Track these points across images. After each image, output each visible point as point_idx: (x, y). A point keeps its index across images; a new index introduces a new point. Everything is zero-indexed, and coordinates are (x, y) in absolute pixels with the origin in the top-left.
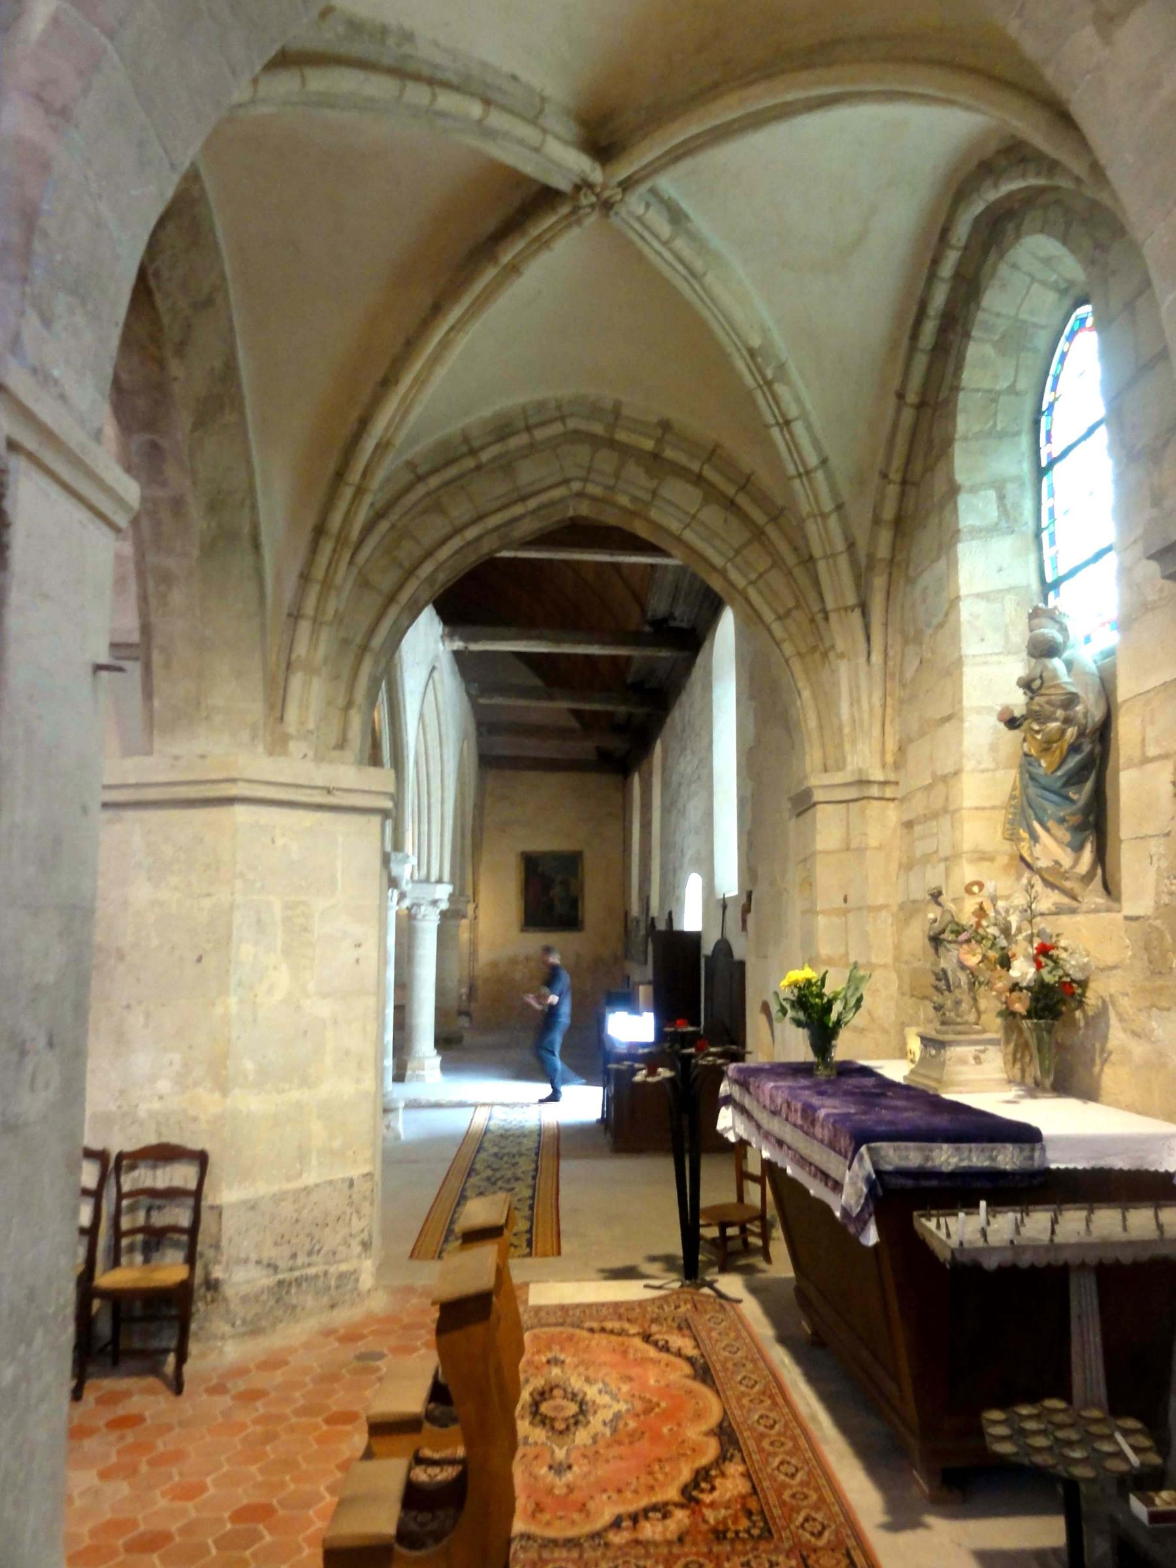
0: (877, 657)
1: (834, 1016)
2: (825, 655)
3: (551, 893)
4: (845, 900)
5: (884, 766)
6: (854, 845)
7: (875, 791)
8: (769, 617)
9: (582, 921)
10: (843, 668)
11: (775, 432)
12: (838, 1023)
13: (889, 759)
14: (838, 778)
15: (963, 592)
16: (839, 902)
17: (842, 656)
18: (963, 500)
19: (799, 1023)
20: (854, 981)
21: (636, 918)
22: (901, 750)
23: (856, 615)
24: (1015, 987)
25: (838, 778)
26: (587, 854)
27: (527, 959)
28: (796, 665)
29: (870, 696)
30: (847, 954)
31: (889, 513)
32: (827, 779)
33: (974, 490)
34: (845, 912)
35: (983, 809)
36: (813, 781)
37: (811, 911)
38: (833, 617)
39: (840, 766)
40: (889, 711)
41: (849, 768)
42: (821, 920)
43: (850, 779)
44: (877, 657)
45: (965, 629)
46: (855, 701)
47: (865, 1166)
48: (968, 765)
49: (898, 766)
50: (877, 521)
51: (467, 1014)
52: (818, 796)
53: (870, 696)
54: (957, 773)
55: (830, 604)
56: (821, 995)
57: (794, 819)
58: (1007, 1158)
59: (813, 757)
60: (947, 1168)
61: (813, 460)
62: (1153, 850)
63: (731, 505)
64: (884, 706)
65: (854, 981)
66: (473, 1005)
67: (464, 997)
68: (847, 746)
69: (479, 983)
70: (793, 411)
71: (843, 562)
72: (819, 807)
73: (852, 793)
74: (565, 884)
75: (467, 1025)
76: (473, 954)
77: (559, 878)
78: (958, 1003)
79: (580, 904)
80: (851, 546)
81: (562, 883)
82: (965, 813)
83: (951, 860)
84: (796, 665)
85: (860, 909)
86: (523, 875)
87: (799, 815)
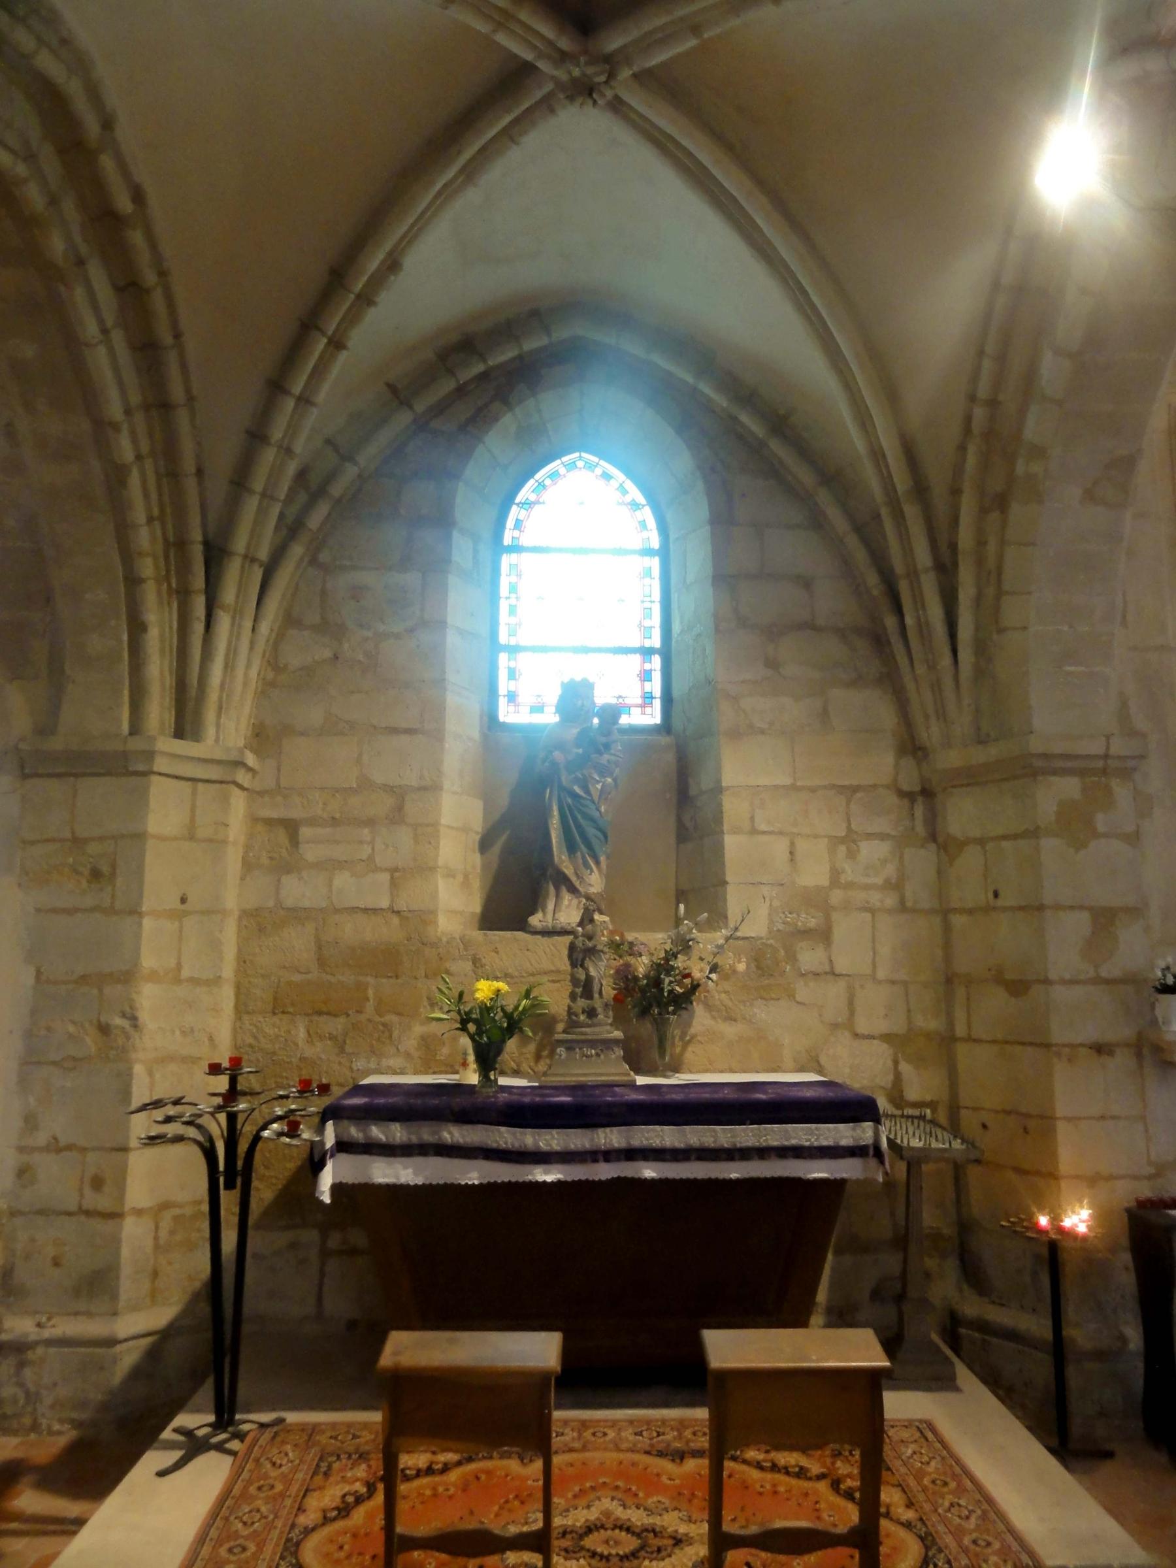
0: (264, 628)
4: (183, 900)
6: (201, 833)
16: (177, 904)
29: (248, 666)
30: (179, 966)
34: (177, 916)
35: (452, 828)
42: (147, 923)
46: (229, 666)
52: (160, 764)
53: (248, 666)
62: (766, 894)
72: (155, 779)
73: (214, 773)
82: (442, 830)
85: (208, 912)
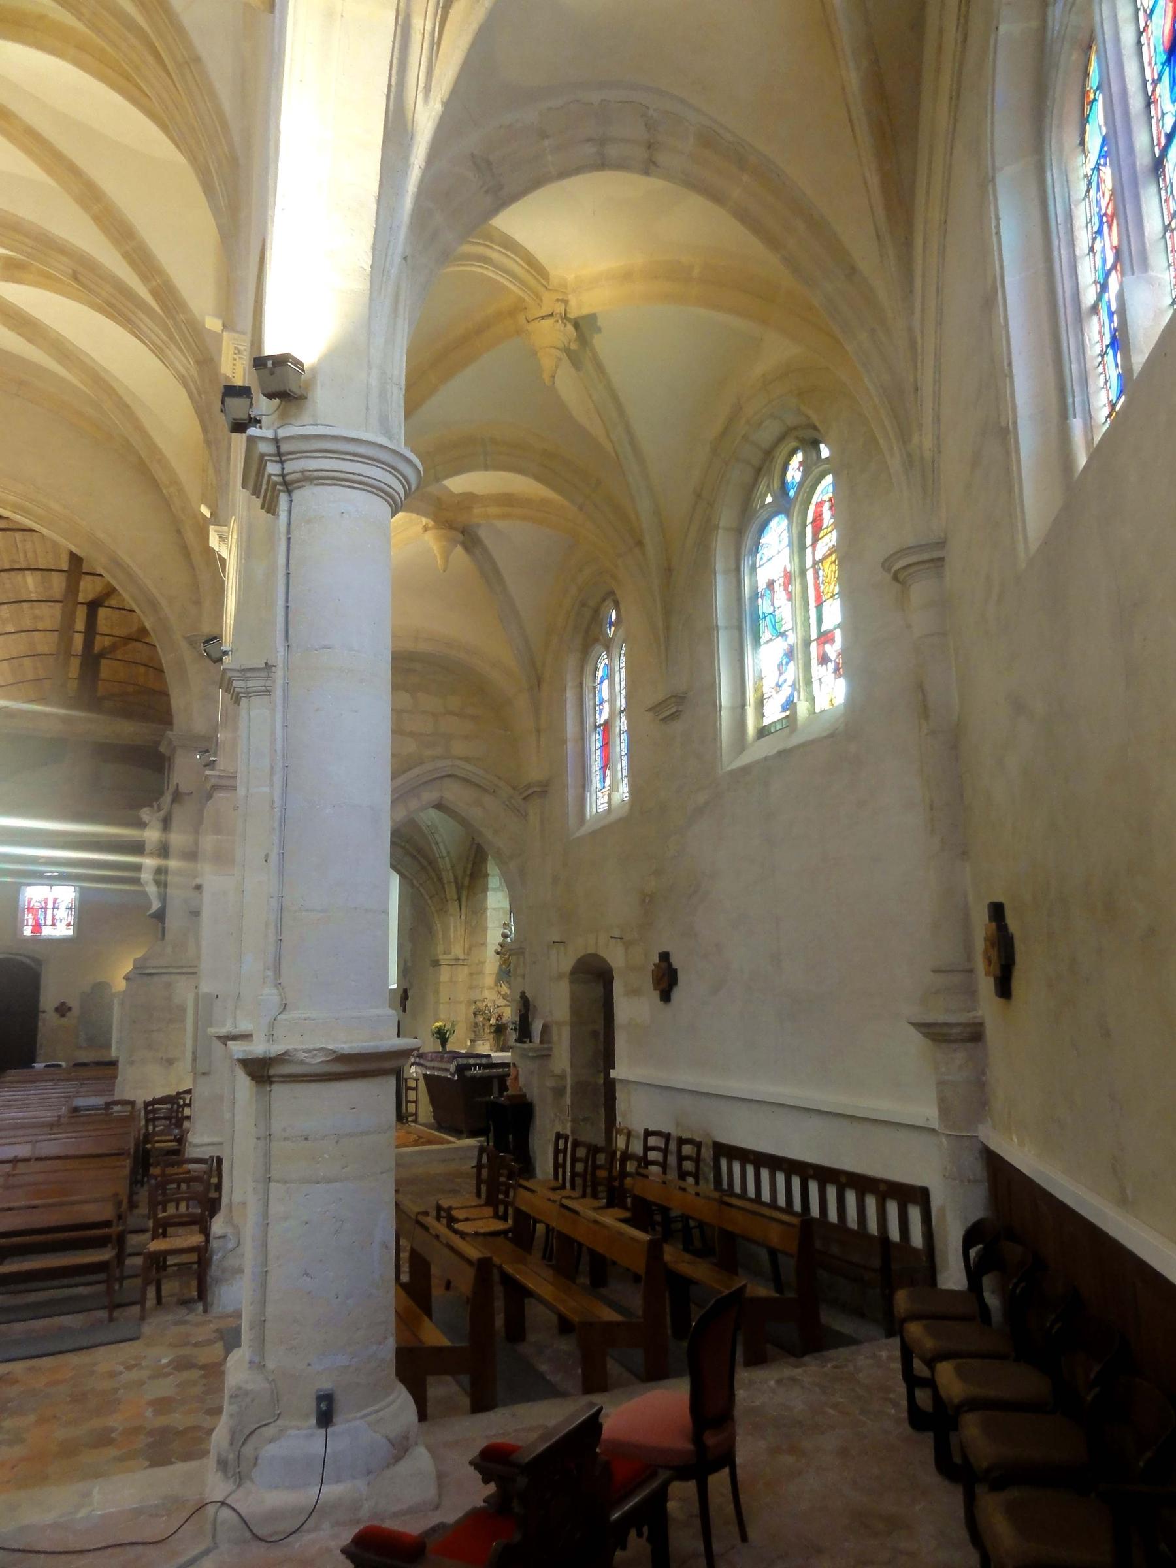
0: (463, 917)
1: (447, 1035)
2: (446, 912)
5: (464, 953)
7: (461, 962)
8: (427, 897)
10: (452, 919)
11: (433, 845)
12: (448, 1037)
13: (466, 951)
14: (449, 957)
15: (489, 907)
16: (448, 1000)
17: (451, 915)
18: (490, 879)
19: (438, 1038)
20: (453, 1026)
22: (470, 949)
23: (457, 902)
24: (491, 1025)
25: (449, 957)
28: (436, 915)
31: (469, 872)
32: (445, 957)
33: (493, 876)
36: (441, 957)
37: (437, 1002)
38: (450, 902)
39: (450, 953)
40: (466, 937)
41: (453, 953)
42: (441, 1006)
43: (453, 958)
44: (463, 917)
45: (489, 919)
47: (455, 1063)
48: (488, 961)
49: (468, 954)
50: (465, 871)
52: (442, 962)
54: (485, 962)
55: (448, 897)
56: (444, 1030)
57: (431, 967)
58: (484, 1061)
59: (440, 948)
60: (472, 1063)
61: (445, 854)
63: (414, 857)
64: (465, 933)
65: (453, 1026)
68: (452, 946)
70: (439, 840)
71: (453, 885)
78: (479, 1030)
80: (456, 879)
83: (482, 988)
84: (436, 915)
87: (434, 966)
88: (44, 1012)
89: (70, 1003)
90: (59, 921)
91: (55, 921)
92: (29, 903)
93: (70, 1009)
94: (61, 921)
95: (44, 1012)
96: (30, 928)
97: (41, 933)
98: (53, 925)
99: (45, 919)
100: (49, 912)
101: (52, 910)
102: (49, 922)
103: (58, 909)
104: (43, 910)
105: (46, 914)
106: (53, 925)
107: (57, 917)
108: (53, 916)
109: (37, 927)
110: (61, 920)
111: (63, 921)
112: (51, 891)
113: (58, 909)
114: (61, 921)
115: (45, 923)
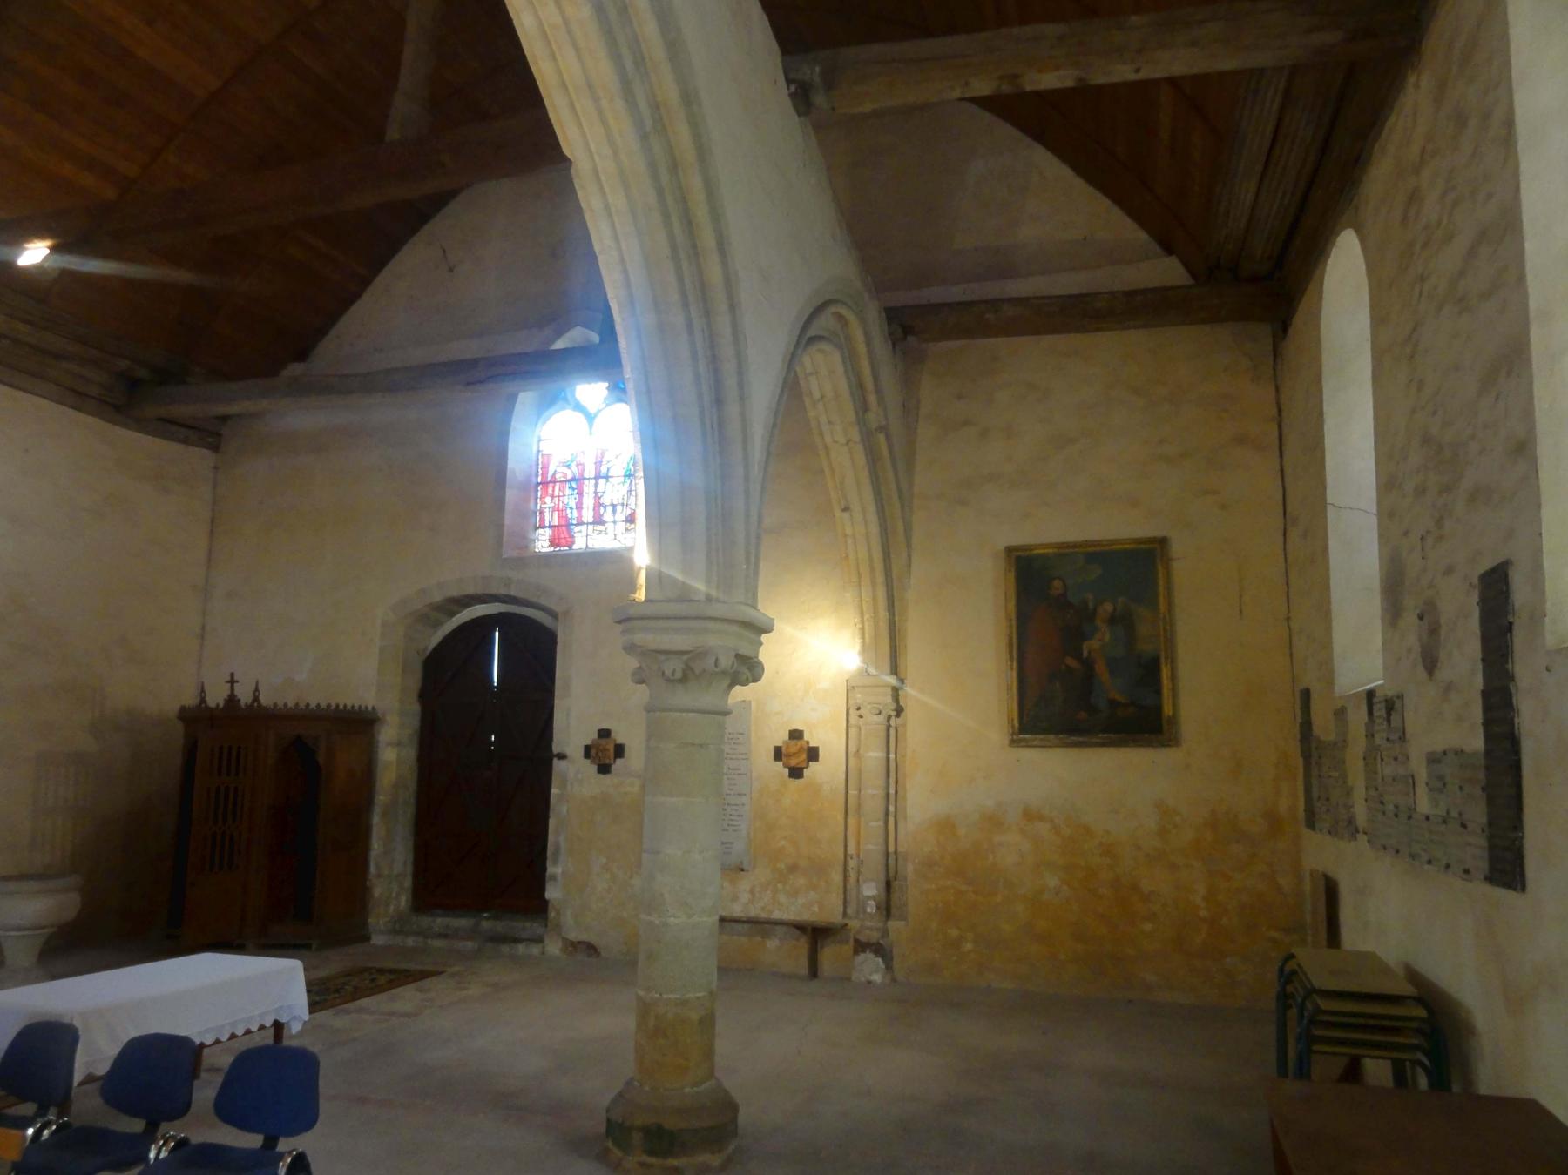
3: (1085, 647)
9: (1174, 721)
21: (1370, 694)
26: (1176, 548)
27: (1030, 815)
51: (879, 950)
66: (893, 924)
67: (871, 908)
69: (909, 870)
74: (1122, 621)
75: (877, 978)
76: (892, 797)
77: (1108, 607)
79: (1165, 673)
81: (1113, 620)
86: (1012, 605)
88: (562, 757)
89: (620, 736)
90: (610, 509)
91: (602, 509)
92: (546, 468)
93: (619, 751)
94: (614, 511)
95: (562, 757)
96: (548, 532)
97: (570, 545)
98: (598, 520)
99: (579, 507)
100: (588, 488)
101: (593, 482)
102: (588, 515)
103: (607, 477)
104: (574, 485)
105: (580, 494)
106: (598, 520)
107: (606, 500)
108: (597, 497)
109: (562, 532)
110: (614, 506)
111: (619, 508)
112: (591, 434)
113: (607, 477)
114: (614, 511)
115: (580, 516)
